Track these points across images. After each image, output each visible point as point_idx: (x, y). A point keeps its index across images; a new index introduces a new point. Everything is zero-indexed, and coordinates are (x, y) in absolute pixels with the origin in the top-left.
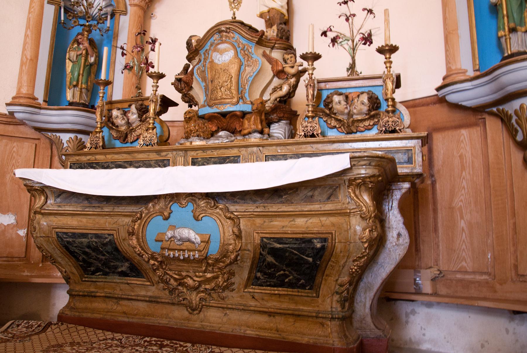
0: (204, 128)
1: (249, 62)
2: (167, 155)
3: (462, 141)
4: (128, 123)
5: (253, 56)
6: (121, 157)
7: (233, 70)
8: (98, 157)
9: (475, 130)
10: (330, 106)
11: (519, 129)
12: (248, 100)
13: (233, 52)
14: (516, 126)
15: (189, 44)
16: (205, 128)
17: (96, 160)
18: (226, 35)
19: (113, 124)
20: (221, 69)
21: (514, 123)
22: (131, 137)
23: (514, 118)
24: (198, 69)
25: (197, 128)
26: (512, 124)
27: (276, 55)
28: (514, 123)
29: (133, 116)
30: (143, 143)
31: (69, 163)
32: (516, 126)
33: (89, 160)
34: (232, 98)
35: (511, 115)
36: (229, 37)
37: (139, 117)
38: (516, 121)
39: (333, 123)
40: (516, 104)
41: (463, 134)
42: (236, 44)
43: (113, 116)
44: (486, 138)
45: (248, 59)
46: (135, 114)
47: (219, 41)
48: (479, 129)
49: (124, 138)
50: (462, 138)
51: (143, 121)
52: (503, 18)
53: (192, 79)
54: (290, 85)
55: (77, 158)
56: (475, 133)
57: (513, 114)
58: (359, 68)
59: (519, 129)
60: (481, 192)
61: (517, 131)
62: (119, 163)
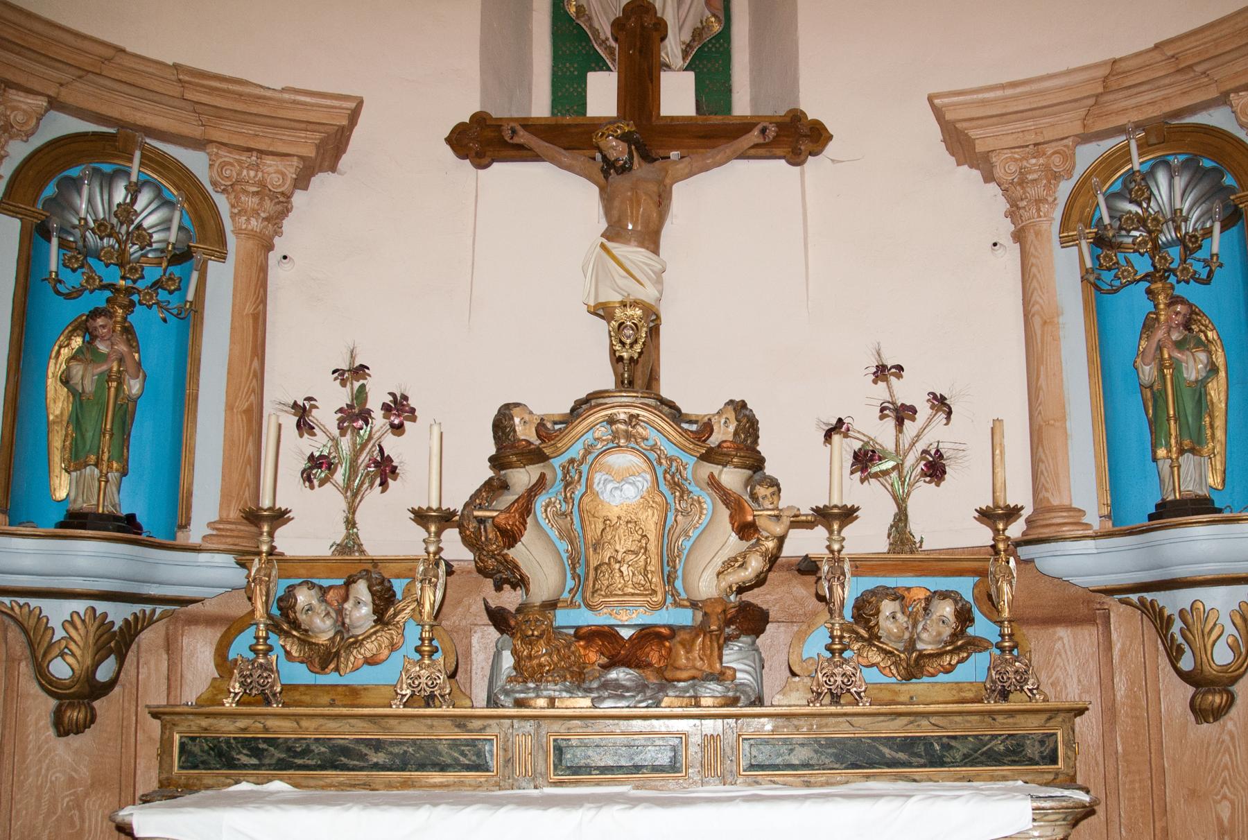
0: (569, 658)
1: (683, 505)
2: (484, 728)
3: (1059, 653)
4: (342, 627)
5: (690, 488)
6: (347, 728)
7: (650, 521)
8: (271, 723)
9: (1086, 632)
10: (872, 624)
11: (1186, 647)
12: (684, 596)
13: (648, 477)
14: (1180, 640)
15: (502, 425)
16: (573, 658)
17: (266, 730)
18: (626, 431)
19: (295, 624)
20: (619, 518)
21: (1178, 636)
22: (348, 660)
23: (1177, 625)
24: (547, 506)
25: (555, 658)
26: (1172, 635)
27: (732, 478)
28: (1178, 636)
29: (361, 612)
30: (409, 692)
31: (177, 737)
32: (1180, 640)
33: (244, 730)
34: (654, 592)
35: (1169, 617)
36: (634, 436)
37: (374, 612)
38: (1181, 630)
39: (876, 658)
40: (1184, 598)
41: (1061, 638)
42: (653, 456)
43: (298, 607)
44: (1109, 648)
45: (682, 496)
46: (366, 605)
47: (611, 445)
48: (1094, 630)
49: (325, 658)
50: (1058, 645)
51: (387, 624)
52: (1168, 420)
53: (524, 523)
54: (764, 555)
55: (204, 723)
56: (1087, 637)
57: (1176, 617)
58: (916, 527)
59: (1186, 647)
60: (1097, 764)
61: (1180, 651)
62: (342, 742)
